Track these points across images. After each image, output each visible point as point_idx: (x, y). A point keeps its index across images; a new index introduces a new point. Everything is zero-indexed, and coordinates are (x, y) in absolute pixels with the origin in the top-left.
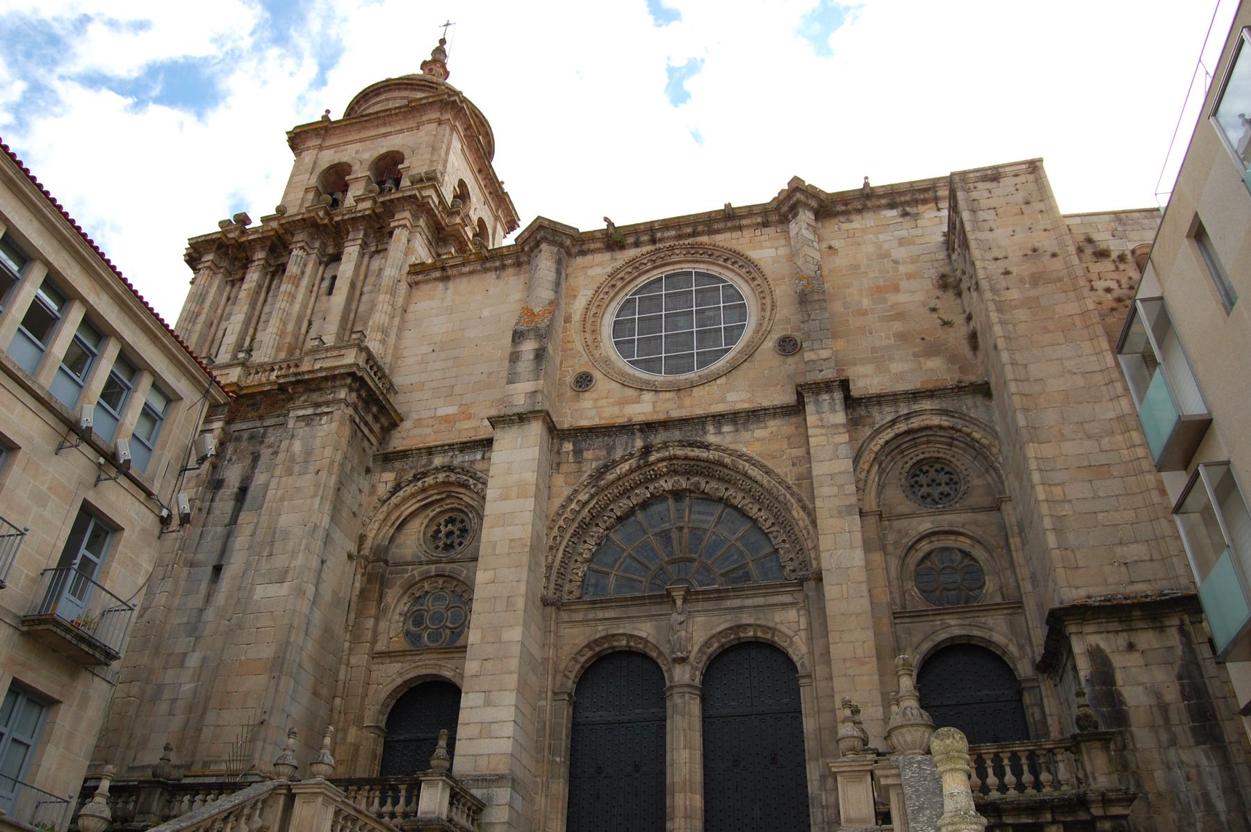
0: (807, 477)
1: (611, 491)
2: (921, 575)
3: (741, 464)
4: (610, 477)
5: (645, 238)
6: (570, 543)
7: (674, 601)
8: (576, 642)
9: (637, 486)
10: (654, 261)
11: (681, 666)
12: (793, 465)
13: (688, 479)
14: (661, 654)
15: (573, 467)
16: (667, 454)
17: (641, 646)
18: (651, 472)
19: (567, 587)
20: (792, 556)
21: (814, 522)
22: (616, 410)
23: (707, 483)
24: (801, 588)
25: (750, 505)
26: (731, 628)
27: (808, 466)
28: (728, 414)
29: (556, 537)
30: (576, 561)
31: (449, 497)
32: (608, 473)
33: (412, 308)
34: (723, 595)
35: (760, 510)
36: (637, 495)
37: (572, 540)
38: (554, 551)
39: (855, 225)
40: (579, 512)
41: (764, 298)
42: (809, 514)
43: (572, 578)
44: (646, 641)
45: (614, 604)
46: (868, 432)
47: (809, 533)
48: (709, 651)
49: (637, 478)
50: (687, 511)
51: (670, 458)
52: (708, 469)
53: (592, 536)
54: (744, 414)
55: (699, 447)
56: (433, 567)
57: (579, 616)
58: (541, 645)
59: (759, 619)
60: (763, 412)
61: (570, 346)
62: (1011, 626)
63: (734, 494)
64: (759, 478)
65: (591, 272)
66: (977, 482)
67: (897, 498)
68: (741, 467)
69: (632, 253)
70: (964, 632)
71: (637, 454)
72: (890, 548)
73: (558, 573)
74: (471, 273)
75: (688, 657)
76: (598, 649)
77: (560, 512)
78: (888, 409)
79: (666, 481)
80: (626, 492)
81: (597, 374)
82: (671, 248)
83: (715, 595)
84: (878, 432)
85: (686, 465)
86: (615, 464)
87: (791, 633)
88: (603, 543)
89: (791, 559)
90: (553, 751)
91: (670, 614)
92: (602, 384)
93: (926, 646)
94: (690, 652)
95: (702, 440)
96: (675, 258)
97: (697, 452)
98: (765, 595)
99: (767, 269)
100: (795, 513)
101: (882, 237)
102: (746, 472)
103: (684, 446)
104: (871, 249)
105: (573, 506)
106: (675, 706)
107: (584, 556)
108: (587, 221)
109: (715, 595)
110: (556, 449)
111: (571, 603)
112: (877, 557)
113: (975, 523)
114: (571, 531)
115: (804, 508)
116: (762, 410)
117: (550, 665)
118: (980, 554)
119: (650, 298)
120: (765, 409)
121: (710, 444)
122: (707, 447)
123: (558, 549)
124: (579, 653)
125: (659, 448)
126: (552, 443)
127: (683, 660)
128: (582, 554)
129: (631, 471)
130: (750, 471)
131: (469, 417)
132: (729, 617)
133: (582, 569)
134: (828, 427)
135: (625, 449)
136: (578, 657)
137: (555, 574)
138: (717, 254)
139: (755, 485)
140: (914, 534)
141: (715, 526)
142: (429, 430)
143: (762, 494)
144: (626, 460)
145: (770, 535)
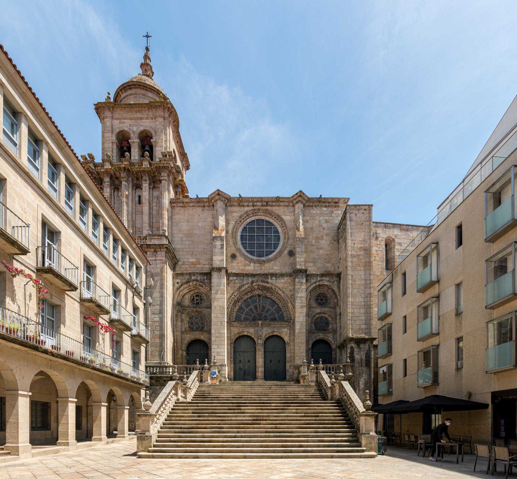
0: (293, 297)
2: (316, 323)
4: (243, 289)
5: (251, 204)
9: (249, 292)
10: (253, 214)
21: (294, 308)
22: (243, 268)
31: (196, 289)
33: (173, 217)
39: (314, 212)
41: (285, 235)
46: (309, 284)
52: (268, 289)
56: (195, 309)
61: (229, 243)
62: (333, 337)
64: (281, 294)
65: (235, 214)
66: (332, 301)
67: (314, 304)
69: (247, 209)
70: (323, 337)
72: (310, 316)
74: (193, 206)
78: (315, 278)
80: (246, 294)
81: (238, 254)
82: (259, 209)
84: (312, 284)
90: (231, 358)
92: (240, 258)
93: (314, 340)
96: (260, 214)
97: (265, 284)
99: (288, 223)
101: (321, 218)
104: (317, 222)
106: (259, 349)
108: (233, 193)
112: (307, 317)
113: (330, 311)
114: (232, 303)
115: (292, 303)
118: (330, 319)
119: (252, 228)
124: (235, 335)
127: (261, 339)
131: (200, 264)
138: (272, 215)
140: (315, 312)
142: (187, 266)
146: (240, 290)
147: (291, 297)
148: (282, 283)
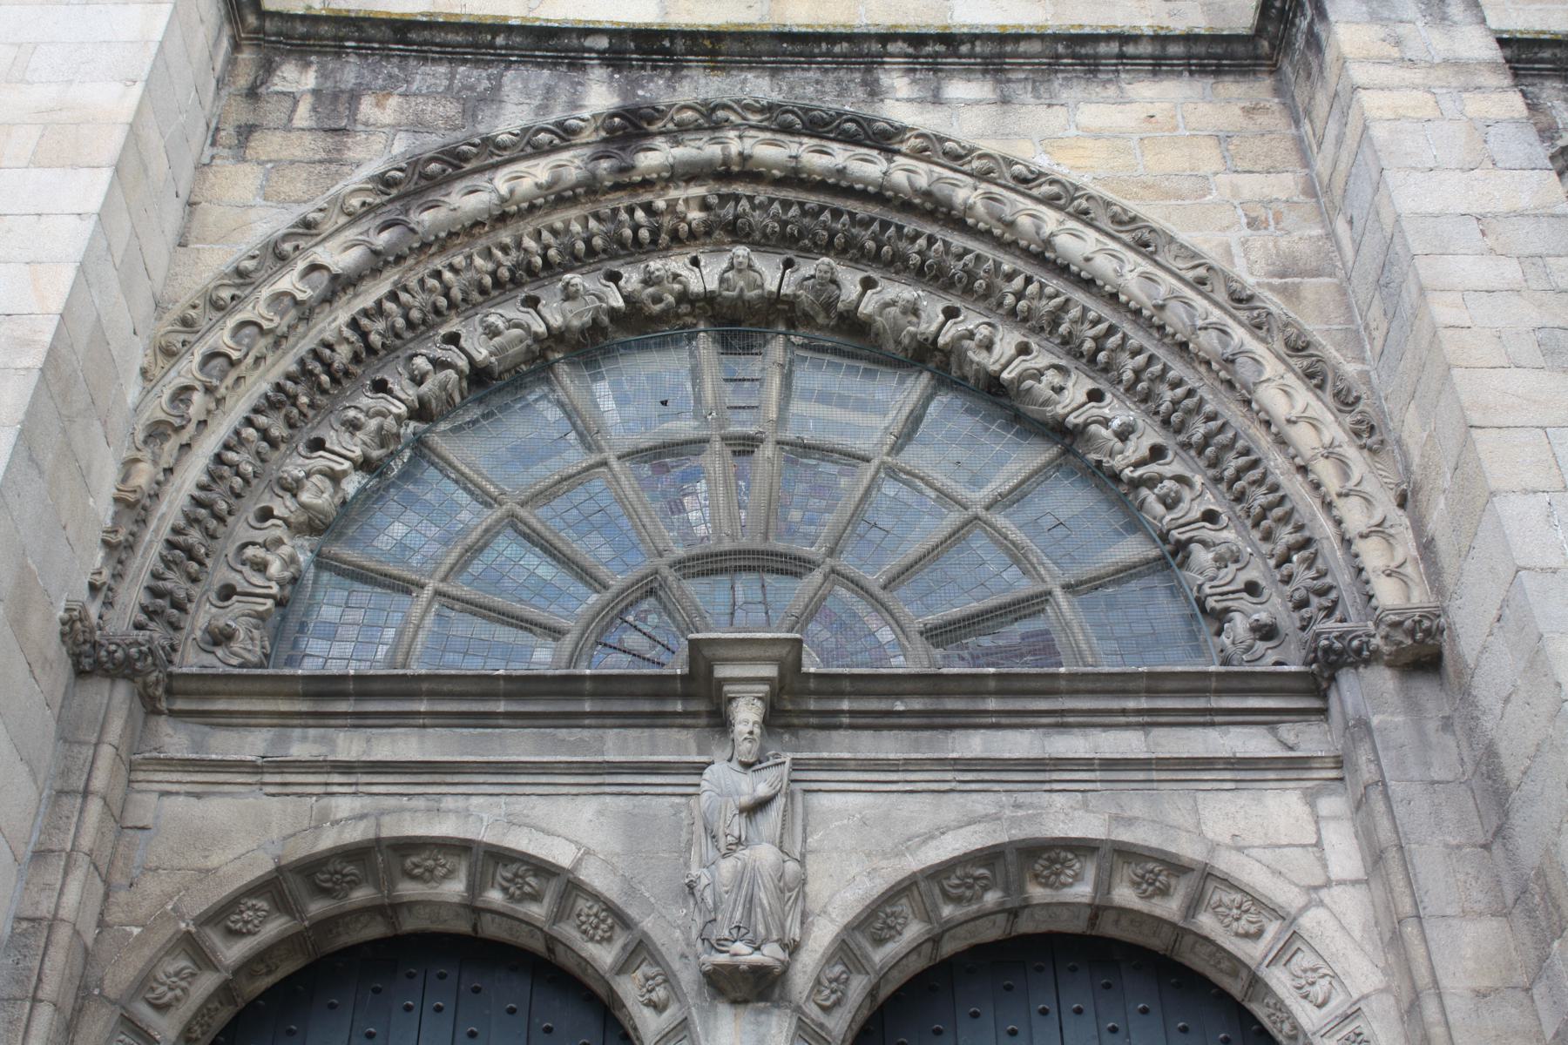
1: (459, 260)
3: (1028, 215)
6: (250, 433)
7: (720, 721)
8: (214, 861)
9: (574, 261)
11: (746, 1013)
12: (1252, 223)
13: (788, 264)
14: (640, 950)
15: (309, 146)
16: (713, 151)
17: (536, 912)
18: (640, 215)
19: (204, 615)
20: (1252, 574)
23: (868, 284)
24: (1315, 703)
25: (1052, 377)
26: (990, 857)
27: (1317, 231)
28: (973, 38)
29: (188, 389)
30: (266, 514)
32: (459, 186)
34: (951, 704)
35: (1095, 396)
36: (569, 295)
37: (261, 420)
38: (172, 445)
40: (306, 312)
42: (1345, 401)
43: (235, 579)
44: (571, 887)
45: (423, 706)
47: (1345, 473)
48: (880, 956)
49: (576, 228)
50: (775, 382)
51: (722, 172)
53: (354, 426)
54: (1036, 47)
55: (850, 139)
57: (252, 745)
58: (26, 852)
59: (1130, 822)
60: (1114, 47)
63: (984, 331)
64: (1104, 266)
68: (1024, 222)
71: (588, 136)
73: (171, 545)
75: (786, 968)
76: (317, 908)
77: (226, 294)
79: (695, 262)
83: (917, 704)
85: (786, 205)
86: (493, 153)
87: (1286, 895)
88: (396, 467)
89: (1252, 588)
91: (699, 769)
94: (793, 948)
95: (866, 111)
98: (1149, 720)
100: (1272, 398)
102: (1048, 243)
103: (787, 129)
105: (288, 281)
107: (305, 497)
109: (917, 704)
110: (243, 82)
111: (207, 685)
114: (260, 385)
115: (1315, 377)
116: (1109, 37)
117: (57, 958)
120: (1124, 38)
121: (900, 131)
122: (883, 139)
123: (186, 447)
124: (222, 915)
125: (683, 127)
126: (231, 62)
128: (292, 488)
129: (558, 197)
130: (1064, 242)
132: (981, 804)
133: (285, 550)
134: (1432, 66)
135: (543, 108)
136: (214, 938)
137: (158, 548)
139: (1079, 297)
141: (896, 449)
143: (1111, 330)
144: (540, 151)
145: (1150, 496)
146: (426, 219)
147: (1283, 291)
148: (1097, 136)
